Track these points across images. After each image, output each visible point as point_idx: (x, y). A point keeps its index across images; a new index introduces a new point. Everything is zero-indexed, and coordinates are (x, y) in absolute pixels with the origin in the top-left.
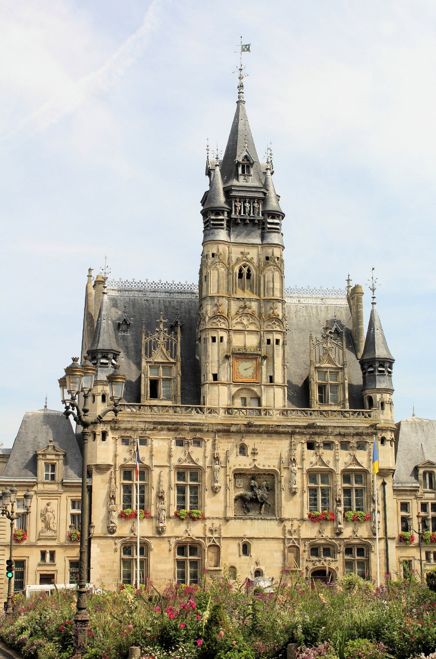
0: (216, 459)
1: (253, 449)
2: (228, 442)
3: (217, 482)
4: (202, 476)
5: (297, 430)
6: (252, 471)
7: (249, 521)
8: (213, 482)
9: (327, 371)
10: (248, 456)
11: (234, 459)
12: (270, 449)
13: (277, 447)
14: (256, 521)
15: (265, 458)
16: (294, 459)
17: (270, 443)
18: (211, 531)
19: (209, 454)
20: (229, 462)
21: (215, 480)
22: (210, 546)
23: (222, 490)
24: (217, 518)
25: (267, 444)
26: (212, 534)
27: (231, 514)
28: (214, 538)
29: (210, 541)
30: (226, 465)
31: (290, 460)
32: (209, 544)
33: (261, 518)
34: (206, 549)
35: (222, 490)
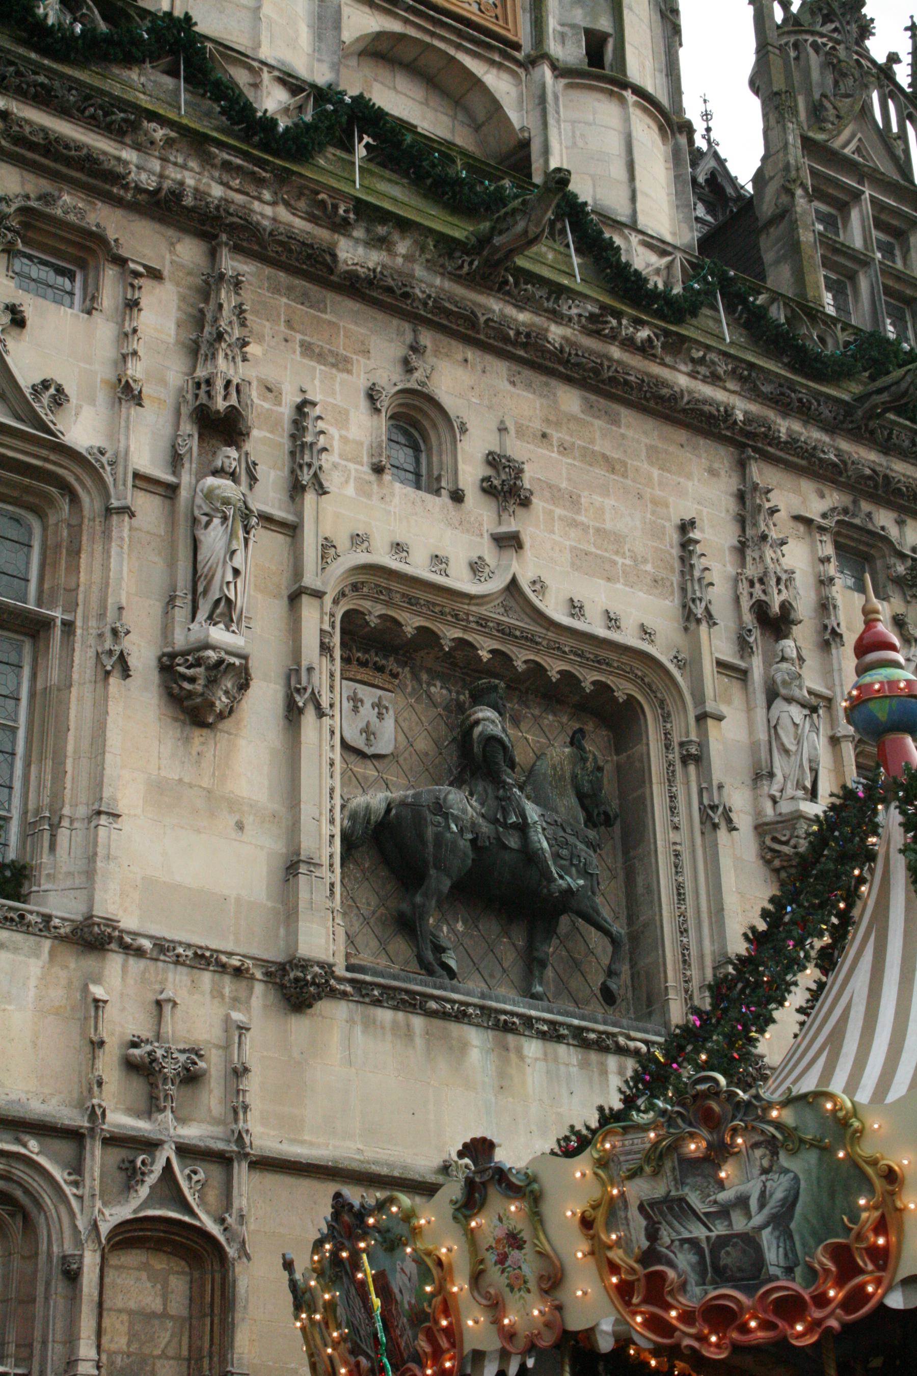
0: (220, 426)
1: (493, 460)
2: (307, 349)
3: (225, 611)
4: (75, 552)
5: (785, 426)
6: (482, 622)
7: (476, 1040)
8: (181, 614)
9: (857, 195)
10: (457, 497)
11: (350, 491)
12: (609, 502)
13: (655, 502)
14: (533, 1048)
15: (581, 560)
16: (786, 607)
17: (611, 465)
18: (142, 1068)
19: (161, 367)
20: (322, 491)
21: (197, 590)
22: (131, 1237)
23: (263, 700)
24: (203, 959)
25: (591, 457)
26: (152, 1106)
27: (321, 938)
28: (168, 1152)
29: (131, 1175)
30: (300, 514)
31: (748, 618)
32: (124, 1212)
33: (578, 1033)
34: (90, 1260)
35: (263, 700)
